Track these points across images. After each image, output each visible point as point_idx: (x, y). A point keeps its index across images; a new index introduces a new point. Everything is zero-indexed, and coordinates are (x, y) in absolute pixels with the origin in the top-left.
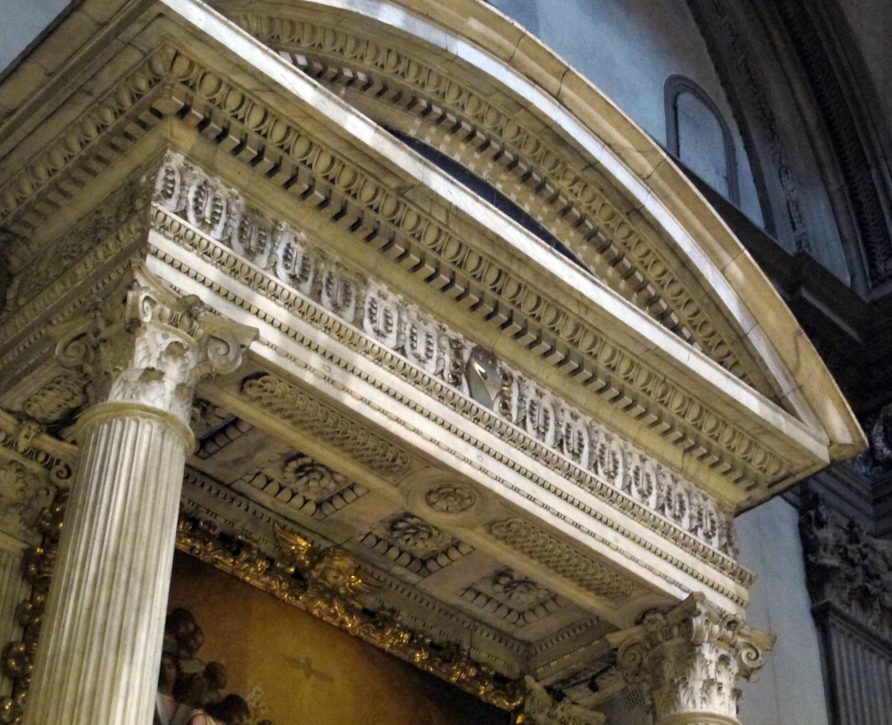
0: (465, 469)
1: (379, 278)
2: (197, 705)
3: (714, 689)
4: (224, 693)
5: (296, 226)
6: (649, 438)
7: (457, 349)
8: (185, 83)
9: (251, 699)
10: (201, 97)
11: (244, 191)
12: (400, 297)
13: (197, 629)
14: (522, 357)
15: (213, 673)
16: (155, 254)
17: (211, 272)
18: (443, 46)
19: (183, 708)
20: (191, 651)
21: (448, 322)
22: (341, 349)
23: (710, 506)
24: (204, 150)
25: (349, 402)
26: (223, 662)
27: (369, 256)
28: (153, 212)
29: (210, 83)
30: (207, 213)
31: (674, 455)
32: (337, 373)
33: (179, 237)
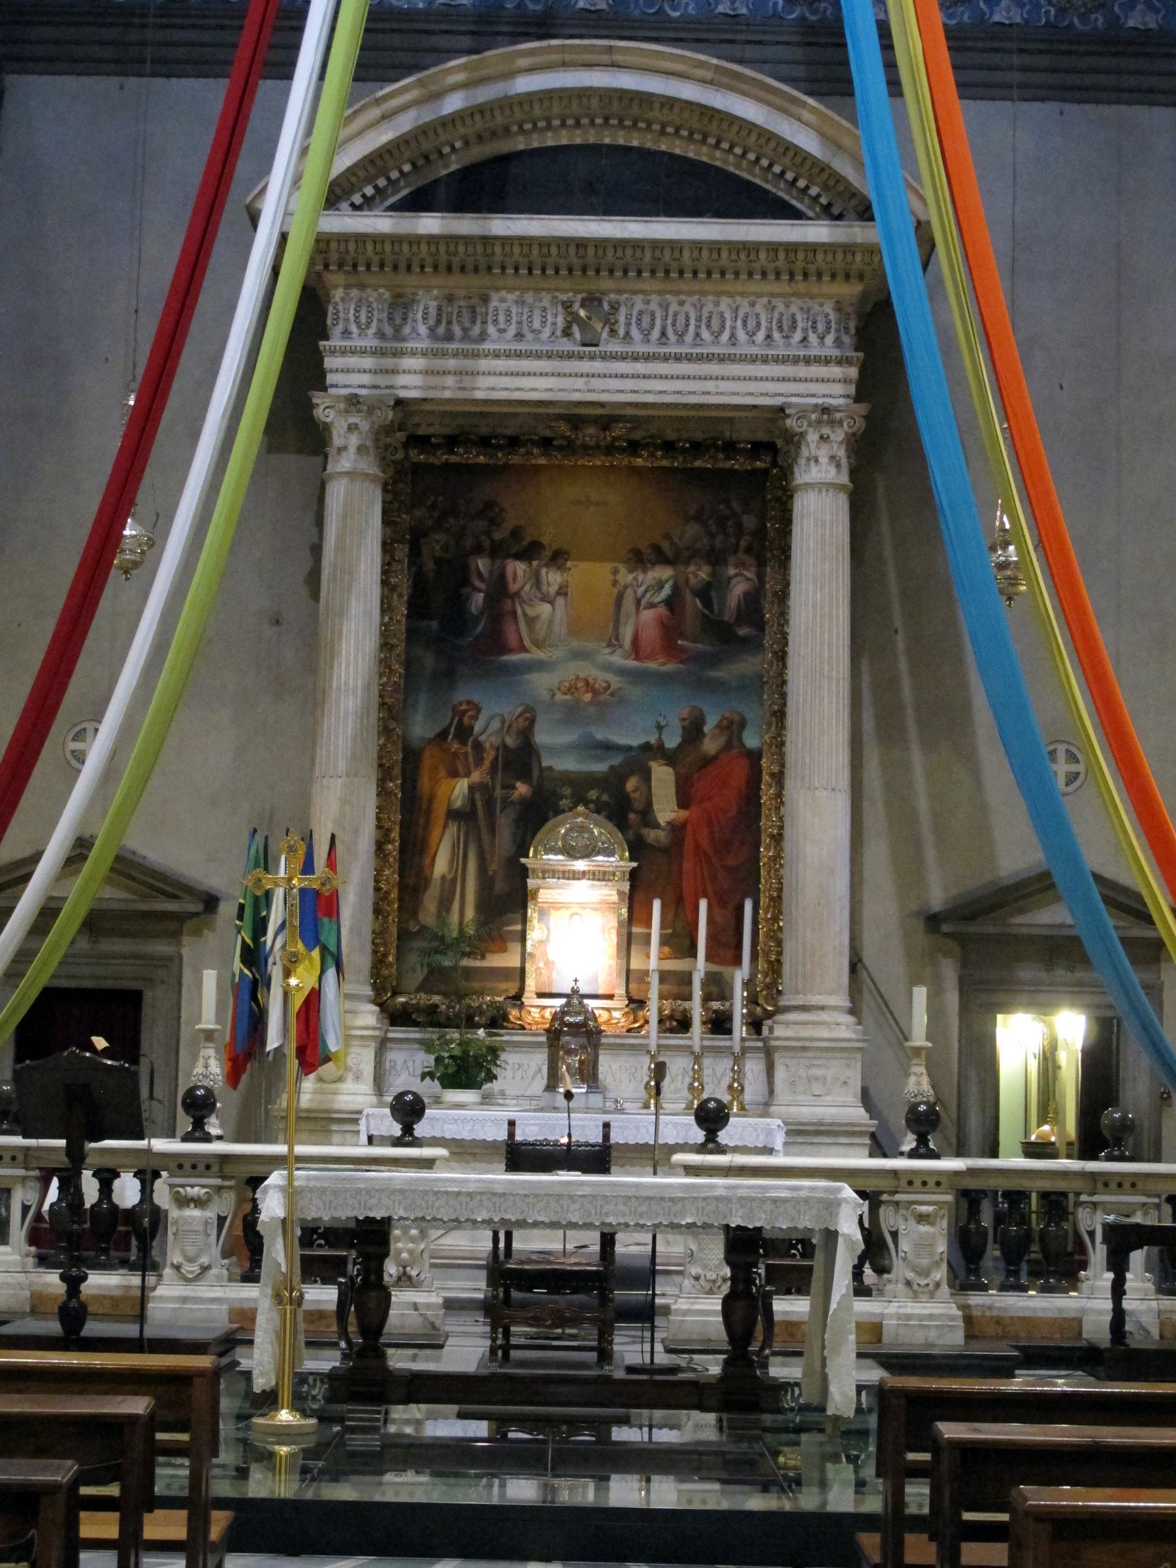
0: (576, 397)
1: (497, 289)
2: (508, 556)
3: (812, 463)
4: (525, 543)
5: (428, 289)
6: (755, 286)
7: (567, 306)
8: (321, 252)
9: (545, 540)
10: (334, 256)
11: (387, 287)
12: (517, 293)
13: (502, 510)
14: (624, 285)
15: (516, 534)
16: (331, 371)
17: (368, 362)
18: (502, 94)
19: (498, 562)
20: (498, 525)
21: (557, 290)
22: (468, 364)
23: (828, 308)
24: (353, 280)
25: (479, 395)
26: (522, 522)
27: (483, 280)
28: (322, 348)
29: (333, 245)
30: (363, 319)
31: (783, 287)
32: (467, 380)
33: (344, 352)
